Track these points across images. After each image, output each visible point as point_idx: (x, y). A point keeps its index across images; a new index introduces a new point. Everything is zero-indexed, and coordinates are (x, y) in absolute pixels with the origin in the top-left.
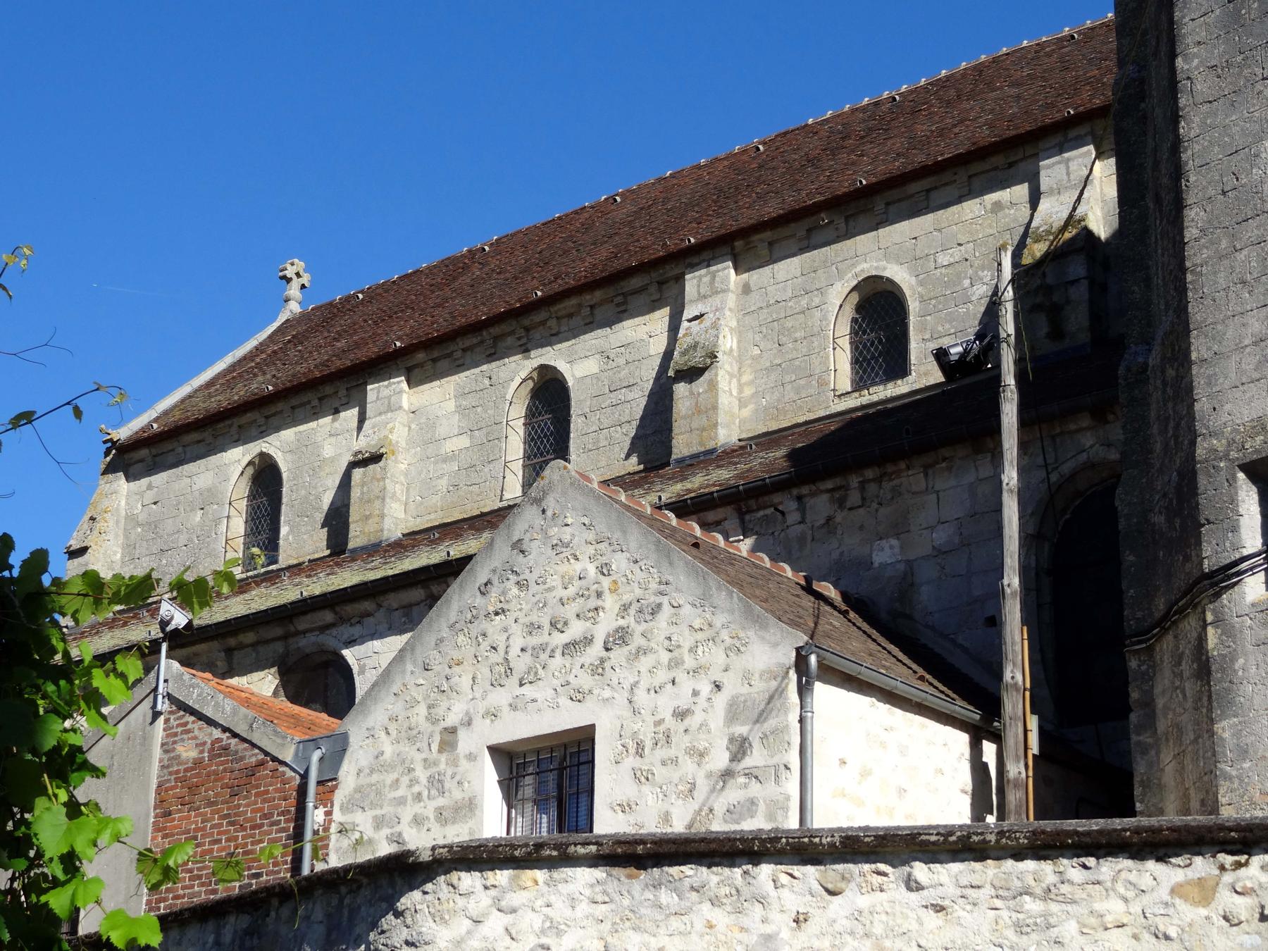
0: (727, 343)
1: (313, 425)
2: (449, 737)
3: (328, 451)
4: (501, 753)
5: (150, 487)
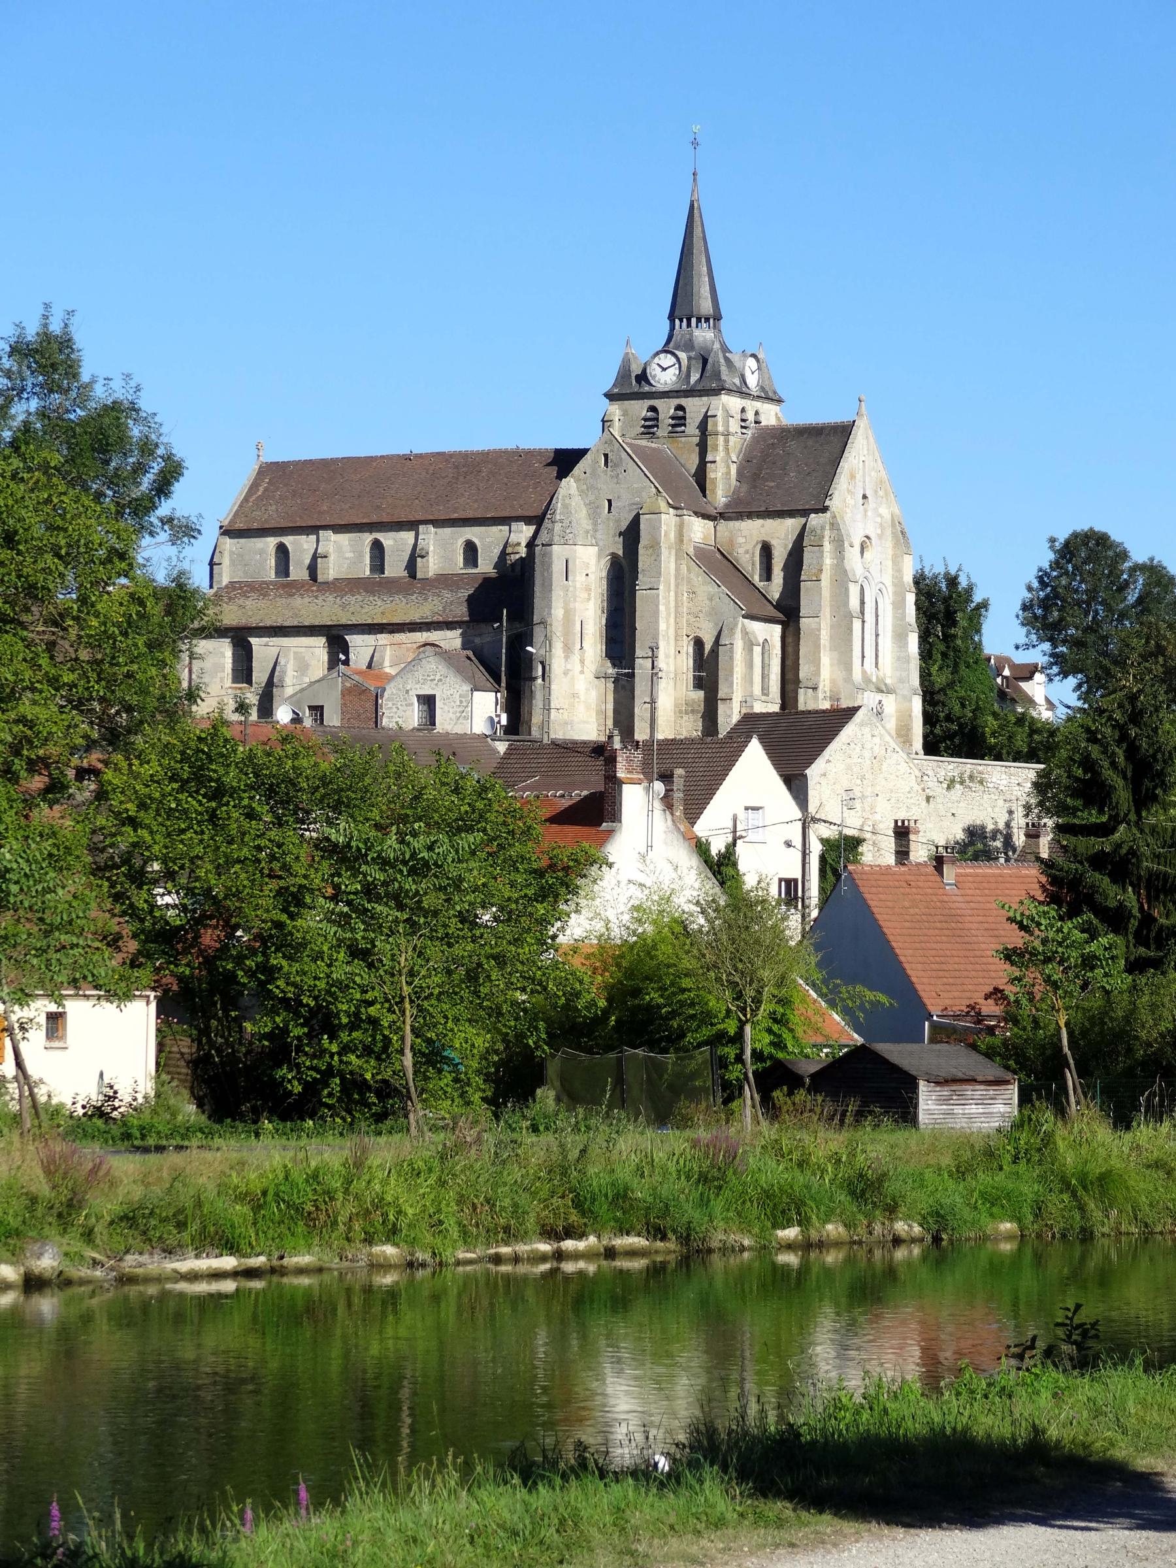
0: (431, 548)
2: (407, 692)
3: (305, 546)
4: (418, 697)
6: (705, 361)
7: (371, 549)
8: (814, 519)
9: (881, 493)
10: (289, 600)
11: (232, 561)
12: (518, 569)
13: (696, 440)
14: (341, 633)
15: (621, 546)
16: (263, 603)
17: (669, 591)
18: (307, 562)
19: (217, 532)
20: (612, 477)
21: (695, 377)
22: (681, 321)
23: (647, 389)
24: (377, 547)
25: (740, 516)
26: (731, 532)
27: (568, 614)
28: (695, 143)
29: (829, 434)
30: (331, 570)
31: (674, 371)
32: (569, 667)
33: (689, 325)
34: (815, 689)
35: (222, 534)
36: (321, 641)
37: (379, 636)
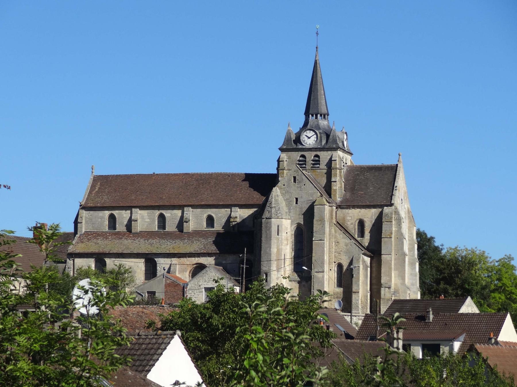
1: (122, 211)
2: (200, 286)
3: (125, 216)
5: (89, 213)
6: (328, 136)
7: (158, 218)
8: (386, 210)
10: (121, 241)
11: (86, 222)
12: (236, 229)
13: (325, 171)
14: (152, 257)
15: (302, 220)
16: (106, 242)
17: (327, 241)
18: (125, 223)
19: (78, 207)
20: (298, 187)
21: (324, 142)
22: (312, 116)
23: (300, 147)
24: (162, 217)
25: (348, 207)
26: (344, 214)
27: (279, 251)
28: (317, 34)
29: (385, 170)
30: (139, 227)
31: (314, 138)
33: (316, 118)
34: (389, 288)
35: (82, 209)
36: (143, 260)
37: (173, 259)
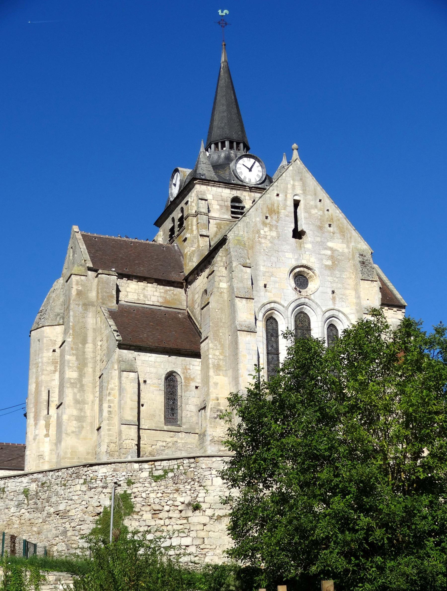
9: (331, 229)
17: (84, 342)
32: (37, 432)
